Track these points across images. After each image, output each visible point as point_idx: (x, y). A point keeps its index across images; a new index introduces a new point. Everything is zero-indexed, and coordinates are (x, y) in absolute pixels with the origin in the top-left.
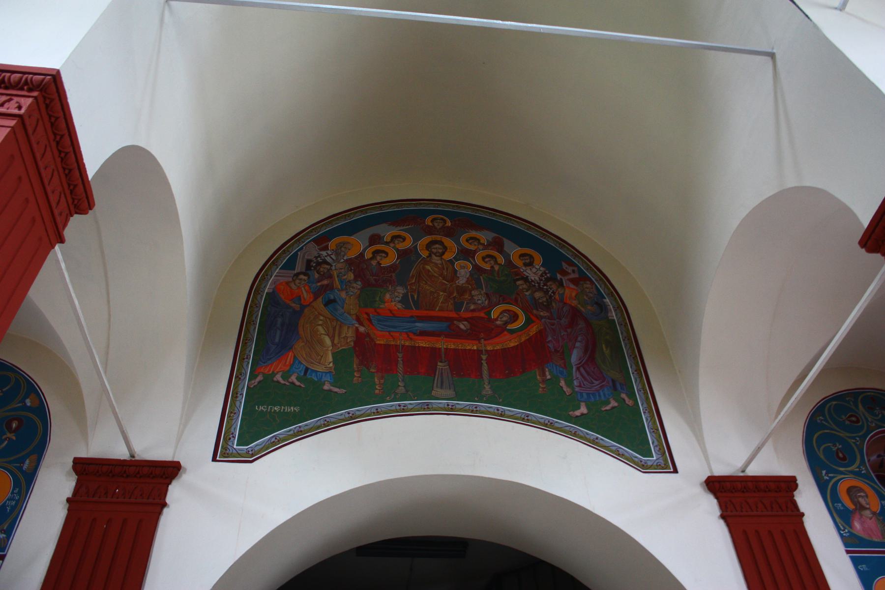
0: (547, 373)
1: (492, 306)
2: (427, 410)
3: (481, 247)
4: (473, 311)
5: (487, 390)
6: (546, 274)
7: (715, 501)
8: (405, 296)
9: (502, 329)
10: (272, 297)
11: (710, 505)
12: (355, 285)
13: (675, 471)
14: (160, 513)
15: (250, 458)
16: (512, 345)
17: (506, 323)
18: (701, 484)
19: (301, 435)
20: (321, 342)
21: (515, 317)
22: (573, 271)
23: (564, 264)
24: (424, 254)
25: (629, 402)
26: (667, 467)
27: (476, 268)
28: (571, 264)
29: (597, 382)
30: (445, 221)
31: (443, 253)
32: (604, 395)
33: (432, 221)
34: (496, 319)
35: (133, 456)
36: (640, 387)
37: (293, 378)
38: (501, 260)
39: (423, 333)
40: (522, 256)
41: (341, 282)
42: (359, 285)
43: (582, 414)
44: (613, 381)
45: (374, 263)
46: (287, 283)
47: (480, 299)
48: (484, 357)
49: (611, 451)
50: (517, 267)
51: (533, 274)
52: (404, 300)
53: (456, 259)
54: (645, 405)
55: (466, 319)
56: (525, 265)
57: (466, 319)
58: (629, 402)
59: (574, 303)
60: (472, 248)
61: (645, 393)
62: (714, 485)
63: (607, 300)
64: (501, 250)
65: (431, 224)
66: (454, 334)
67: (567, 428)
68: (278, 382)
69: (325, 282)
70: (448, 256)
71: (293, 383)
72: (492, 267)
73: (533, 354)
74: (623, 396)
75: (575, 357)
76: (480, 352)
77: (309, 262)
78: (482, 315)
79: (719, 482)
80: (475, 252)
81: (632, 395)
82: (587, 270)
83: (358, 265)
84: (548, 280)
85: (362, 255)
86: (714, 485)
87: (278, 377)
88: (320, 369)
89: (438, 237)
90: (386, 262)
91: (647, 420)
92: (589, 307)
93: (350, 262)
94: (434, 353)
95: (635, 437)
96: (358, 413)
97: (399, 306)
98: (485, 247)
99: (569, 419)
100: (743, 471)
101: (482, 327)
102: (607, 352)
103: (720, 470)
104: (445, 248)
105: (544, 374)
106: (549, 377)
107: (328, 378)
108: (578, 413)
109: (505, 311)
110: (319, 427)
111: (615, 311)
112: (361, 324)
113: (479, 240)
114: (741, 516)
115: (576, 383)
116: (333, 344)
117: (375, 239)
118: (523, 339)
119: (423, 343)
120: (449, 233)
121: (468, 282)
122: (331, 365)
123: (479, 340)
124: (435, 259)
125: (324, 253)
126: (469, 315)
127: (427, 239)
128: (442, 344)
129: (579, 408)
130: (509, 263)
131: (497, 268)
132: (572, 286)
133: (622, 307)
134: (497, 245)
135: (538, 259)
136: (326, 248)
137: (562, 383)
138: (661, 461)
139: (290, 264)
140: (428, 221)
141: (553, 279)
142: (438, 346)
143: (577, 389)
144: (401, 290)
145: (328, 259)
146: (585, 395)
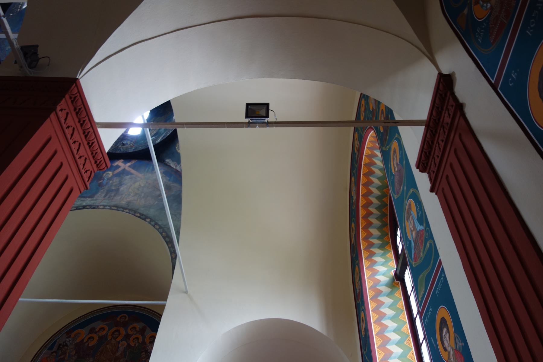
3: (135, 333)
24: (109, 338)
27: (129, 346)
30: (125, 317)
31: (117, 337)
38: (141, 340)
53: (122, 340)
64: (143, 335)
69: (62, 357)
72: (135, 345)
77: (60, 345)
80: (132, 335)
85: (83, 340)
90: (92, 344)
104: (120, 334)
117: (92, 331)
124: (113, 341)
125: (68, 340)
134: (142, 332)
136: (69, 337)
139: (51, 348)
140: (118, 319)
145: (68, 343)
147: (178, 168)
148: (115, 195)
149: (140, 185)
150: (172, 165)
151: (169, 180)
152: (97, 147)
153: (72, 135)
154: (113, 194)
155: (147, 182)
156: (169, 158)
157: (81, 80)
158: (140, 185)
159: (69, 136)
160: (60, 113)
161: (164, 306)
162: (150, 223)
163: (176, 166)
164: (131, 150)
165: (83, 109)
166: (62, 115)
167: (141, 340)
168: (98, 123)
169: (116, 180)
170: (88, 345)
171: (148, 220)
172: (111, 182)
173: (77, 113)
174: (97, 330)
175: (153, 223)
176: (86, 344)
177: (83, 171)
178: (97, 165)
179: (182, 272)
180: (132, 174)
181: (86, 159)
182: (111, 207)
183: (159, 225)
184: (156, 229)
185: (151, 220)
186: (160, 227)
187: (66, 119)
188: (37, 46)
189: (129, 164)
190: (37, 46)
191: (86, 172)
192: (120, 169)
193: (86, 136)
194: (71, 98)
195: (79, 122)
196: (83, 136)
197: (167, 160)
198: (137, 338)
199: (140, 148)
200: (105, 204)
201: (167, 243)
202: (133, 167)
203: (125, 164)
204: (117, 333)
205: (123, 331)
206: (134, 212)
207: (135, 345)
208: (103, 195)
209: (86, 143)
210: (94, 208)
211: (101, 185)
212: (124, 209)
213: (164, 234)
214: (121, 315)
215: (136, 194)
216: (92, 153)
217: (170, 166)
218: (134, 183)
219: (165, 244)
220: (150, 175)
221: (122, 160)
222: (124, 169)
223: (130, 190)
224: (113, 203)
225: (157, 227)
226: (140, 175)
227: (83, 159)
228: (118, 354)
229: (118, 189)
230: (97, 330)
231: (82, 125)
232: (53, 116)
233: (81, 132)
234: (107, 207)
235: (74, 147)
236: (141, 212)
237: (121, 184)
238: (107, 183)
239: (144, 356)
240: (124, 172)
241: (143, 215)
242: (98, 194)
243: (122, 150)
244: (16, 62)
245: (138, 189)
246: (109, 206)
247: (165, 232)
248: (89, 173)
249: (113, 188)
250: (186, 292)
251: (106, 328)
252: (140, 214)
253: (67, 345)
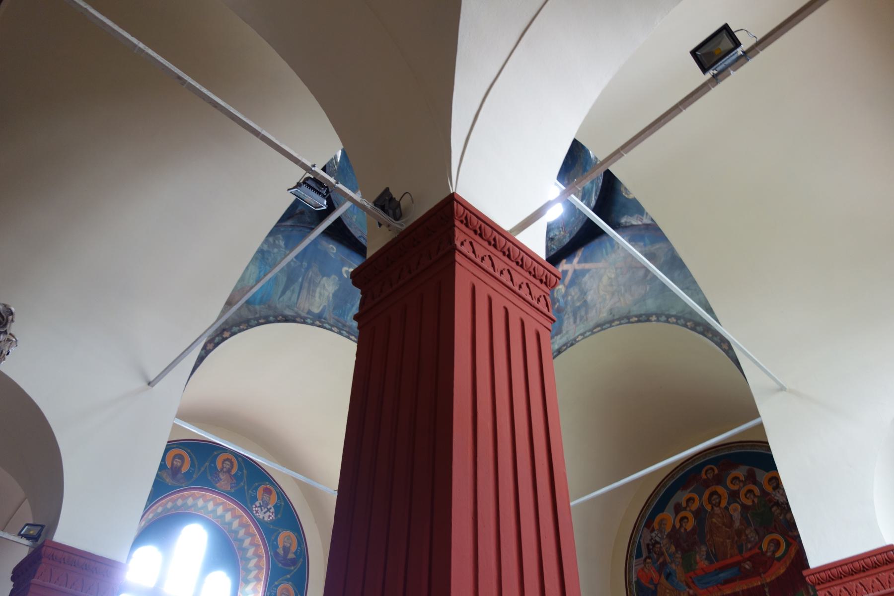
1: (761, 540)
4: (751, 549)
16: (782, 571)
17: (774, 552)
21: (778, 544)
24: (708, 508)
27: (744, 507)
30: (714, 471)
31: (720, 502)
33: (706, 474)
34: (767, 552)
38: (757, 491)
39: (727, 582)
40: (770, 480)
41: (669, 556)
42: (679, 555)
46: (642, 569)
48: (767, 590)
52: (708, 558)
53: (729, 504)
55: (749, 559)
60: (736, 488)
64: (755, 482)
66: (744, 575)
69: (661, 560)
70: (724, 503)
72: (753, 501)
76: (763, 586)
77: (648, 545)
78: (757, 550)
80: (739, 491)
83: (674, 536)
85: (674, 526)
89: (713, 488)
90: (690, 525)
93: (669, 536)
97: (707, 563)
98: (745, 483)
104: (720, 496)
112: (690, 588)
117: (678, 508)
118: (788, 564)
121: (741, 524)
123: (760, 575)
125: (653, 534)
130: (763, 491)
131: (756, 500)
134: (751, 478)
136: (653, 530)
139: (639, 555)
140: (704, 476)
142: (737, 590)
145: (658, 539)
147: (646, 221)
148: (587, 313)
149: (610, 278)
150: (634, 223)
151: (645, 245)
152: (530, 260)
153: (493, 266)
154: (583, 313)
155: (616, 269)
156: (624, 215)
157: (458, 192)
158: (610, 278)
159: (491, 270)
160: (463, 249)
161: (761, 426)
162: (658, 320)
163: (641, 220)
164: (567, 240)
165: (483, 225)
166: (466, 249)
167: (757, 491)
168: (511, 231)
169: (574, 292)
170: (686, 530)
171: (654, 318)
172: (569, 298)
173: (481, 235)
174: (684, 505)
175: (663, 318)
176: (682, 530)
177: (535, 302)
178: (546, 283)
179: (756, 362)
180: (588, 270)
181: (527, 284)
182: (592, 331)
183: (673, 316)
184: (673, 323)
185: (658, 316)
186: (678, 318)
187: (474, 252)
188: (387, 190)
189: (576, 260)
190: (387, 190)
191: (539, 300)
192: (570, 274)
193: (509, 256)
194: (462, 222)
195: (490, 244)
196: (506, 259)
197: (623, 220)
198: (750, 491)
199: (577, 229)
200: (582, 331)
201: (703, 333)
202: (584, 260)
203: (571, 263)
204: (715, 497)
205: (720, 489)
206: (627, 318)
207: (753, 501)
208: (572, 320)
209: (514, 265)
210: (572, 345)
211: (559, 311)
212: (610, 323)
213: (689, 324)
214: (705, 468)
215: (613, 294)
216: (530, 273)
217: (633, 226)
218: (600, 279)
219: (701, 336)
220: (613, 256)
221: (564, 261)
222: (575, 271)
223: (602, 293)
224: (591, 324)
225: (673, 320)
226: (600, 265)
227: (524, 286)
228: (737, 524)
229: (585, 301)
230: (684, 505)
231: (495, 246)
232: (458, 257)
233: (500, 254)
234: (588, 334)
235: (505, 278)
236: (638, 313)
237: (584, 293)
238: (566, 303)
239: (778, 511)
240: (578, 275)
241: (641, 316)
242: (566, 322)
243: (556, 247)
244: (380, 225)
245: (611, 285)
246: (589, 331)
247: (690, 320)
248: (542, 299)
249: (578, 304)
250: (782, 388)
251: (696, 497)
252: (636, 316)
253: (657, 542)
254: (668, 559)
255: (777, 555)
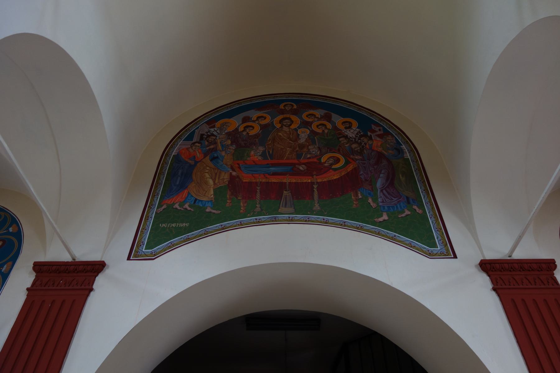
0: (359, 195)
1: (322, 155)
2: (275, 221)
3: (316, 119)
4: (310, 158)
5: (317, 207)
6: (360, 133)
7: (488, 278)
8: (264, 152)
9: (329, 168)
10: (177, 158)
11: (483, 282)
12: (231, 147)
13: (455, 257)
14: (88, 295)
15: (153, 257)
16: (335, 178)
17: (331, 165)
18: (476, 266)
19: (188, 241)
20: (206, 183)
21: (338, 160)
22: (380, 130)
23: (372, 125)
24: (278, 126)
25: (420, 211)
26: (449, 254)
27: (313, 132)
28: (377, 125)
29: (396, 199)
30: (293, 106)
31: (291, 125)
32: (401, 207)
33: (284, 106)
34: (325, 163)
35: (74, 259)
36: (427, 200)
37: (187, 206)
39: (275, 174)
41: (222, 146)
43: (384, 220)
44: (407, 198)
45: (245, 133)
46: (187, 149)
47: (314, 150)
48: (315, 186)
49: (406, 244)
50: (340, 130)
51: (351, 134)
52: (263, 155)
53: (299, 127)
54: (431, 213)
55: (304, 164)
56: (346, 128)
57: (304, 164)
58: (419, 211)
59: (380, 149)
60: (310, 120)
61: (432, 205)
62: (487, 266)
63: (404, 147)
65: (283, 108)
66: (295, 173)
67: (374, 230)
68: (176, 208)
69: (212, 147)
70: (293, 126)
71: (186, 209)
72: (323, 131)
73: (351, 182)
74: (415, 207)
75: (379, 184)
76: (312, 183)
77: (202, 135)
78: (315, 160)
79: (490, 264)
80: (312, 123)
81: (421, 206)
82: (389, 128)
83: (234, 136)
84: (361, 136)
85: (237, 129)
86: (487, 266)
87: (177, 206)
88: (205, 199)
90: (252, 133)
91: (433, 222)
92: (390, 152)
93: (229, 134)
94: (282, 186)
95: (423, 232)
96: (228, 225)
97: (260, 158)
98: (319, 119)
99: (374, 223)
100: (510, 256)
101: (315, 168)
102: (403, 179)
103: (490, 256)
104: (292, 122)
105: (357, 195)
106: (360, 197)
107: (210, 204)
108: (381, 219)
109: (331, 157)
110: (201, 235)
111: (409, 153)
112: (234, 170)
113: (315, 115)
114: (509, 289)
115: (380, 200)
116: (215, 184)
117: (245, 120)
118: (343, 174)
119: (274, 180)
120: (295, 112)
121: (306, 141)
122: (212, 196)
123: (312, 176)
124: (285, 129)
125: (212, 130)
126: (306, 161)
127: (281, 117)
128: (287, 180)
129: (382, 216)
130: (335, 128)
131: (326, 131)
132: (378, 139)
133: (414, 150)
134: (328, 118)
135: (355, 124)
136: (214, 127)
137: (370, 201)
138: (444, 251)
140: (282, 107)
141: (365, 135)
142: (284, 181)
143: (381, 204)
144: (261, 149)
145: (215, 133)
146: (386, 208)
207: (323, 131)
228: (302, 141)
253: (213, 135)
254: (220, 147)
255: (334, 167)
